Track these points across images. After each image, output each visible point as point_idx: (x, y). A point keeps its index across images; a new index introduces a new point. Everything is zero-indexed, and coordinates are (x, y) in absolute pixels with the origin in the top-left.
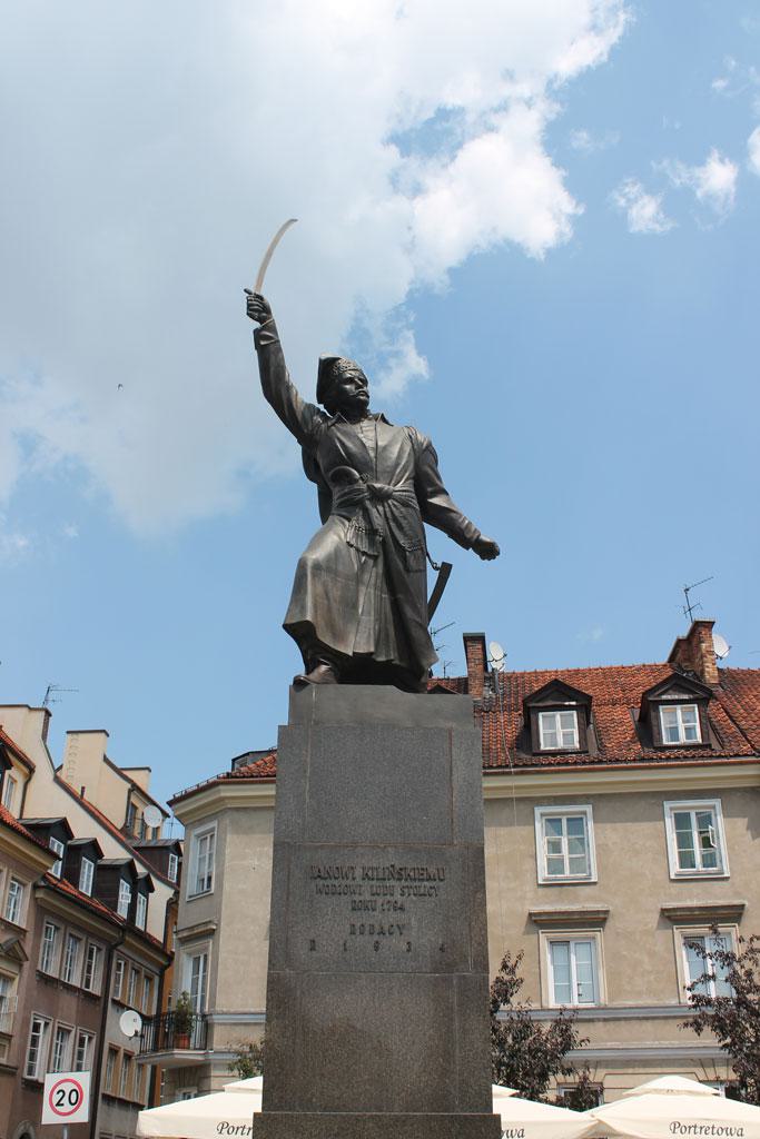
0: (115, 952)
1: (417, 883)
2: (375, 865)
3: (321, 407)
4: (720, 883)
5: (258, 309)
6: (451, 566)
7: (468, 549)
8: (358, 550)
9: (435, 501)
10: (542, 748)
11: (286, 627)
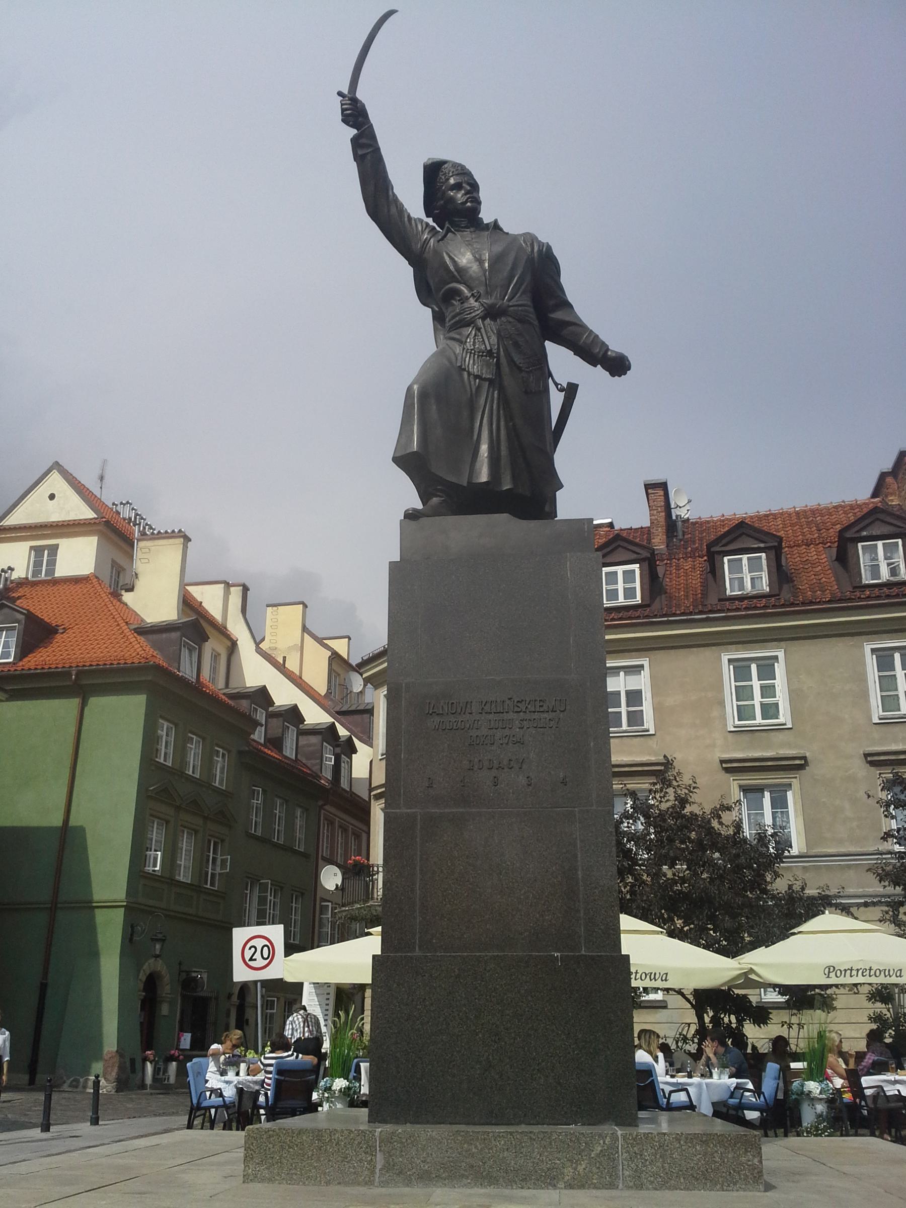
0: (323, 811)
1: (536, 716)
2: (494, 699)
3: (430, 221)
5: (355, 114)
6: (578, 385)
7: (596, 366)
8: (469, 374)
9: (559, 315)
10: (728, 592)
11: (395, 460)
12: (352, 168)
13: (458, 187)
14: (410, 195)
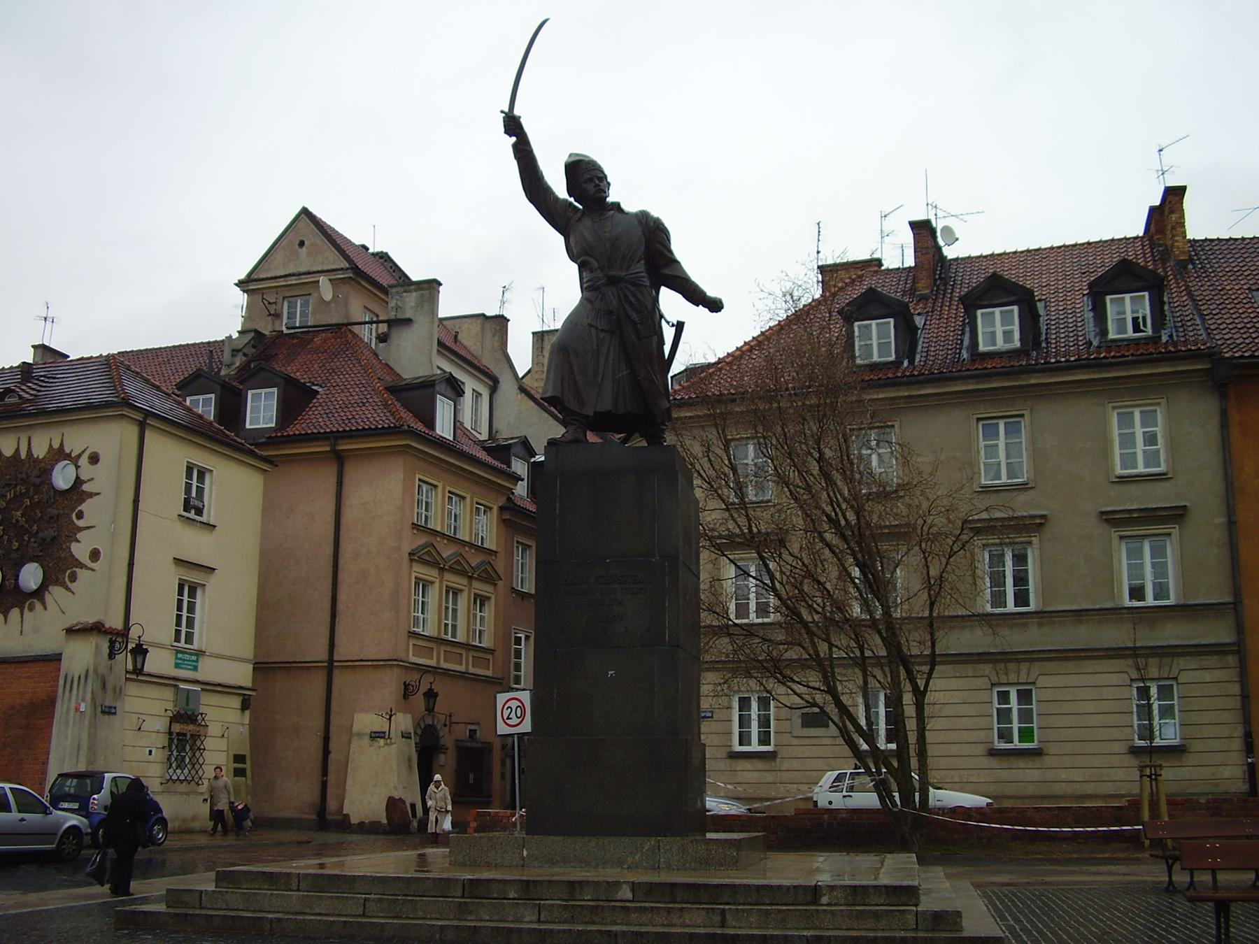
3: (572, 200)
4: (1162, 484)
12: (514, 165)
13: (591, 180)
14: (558, 184)
